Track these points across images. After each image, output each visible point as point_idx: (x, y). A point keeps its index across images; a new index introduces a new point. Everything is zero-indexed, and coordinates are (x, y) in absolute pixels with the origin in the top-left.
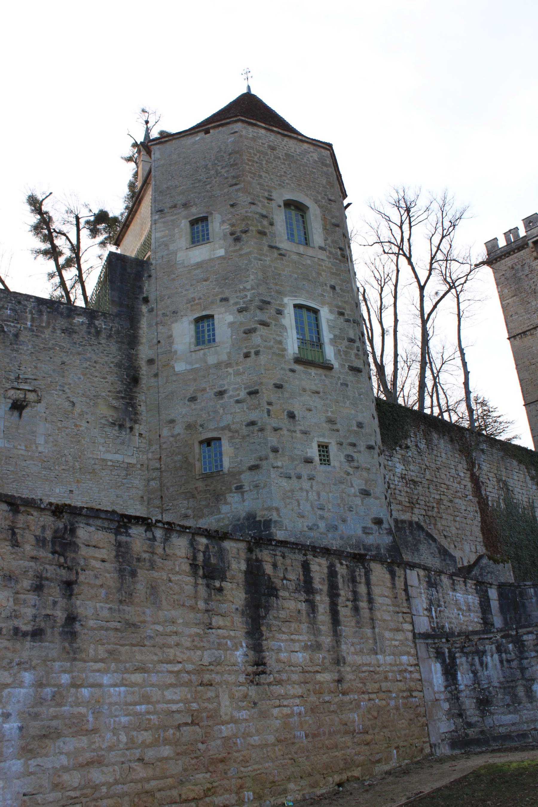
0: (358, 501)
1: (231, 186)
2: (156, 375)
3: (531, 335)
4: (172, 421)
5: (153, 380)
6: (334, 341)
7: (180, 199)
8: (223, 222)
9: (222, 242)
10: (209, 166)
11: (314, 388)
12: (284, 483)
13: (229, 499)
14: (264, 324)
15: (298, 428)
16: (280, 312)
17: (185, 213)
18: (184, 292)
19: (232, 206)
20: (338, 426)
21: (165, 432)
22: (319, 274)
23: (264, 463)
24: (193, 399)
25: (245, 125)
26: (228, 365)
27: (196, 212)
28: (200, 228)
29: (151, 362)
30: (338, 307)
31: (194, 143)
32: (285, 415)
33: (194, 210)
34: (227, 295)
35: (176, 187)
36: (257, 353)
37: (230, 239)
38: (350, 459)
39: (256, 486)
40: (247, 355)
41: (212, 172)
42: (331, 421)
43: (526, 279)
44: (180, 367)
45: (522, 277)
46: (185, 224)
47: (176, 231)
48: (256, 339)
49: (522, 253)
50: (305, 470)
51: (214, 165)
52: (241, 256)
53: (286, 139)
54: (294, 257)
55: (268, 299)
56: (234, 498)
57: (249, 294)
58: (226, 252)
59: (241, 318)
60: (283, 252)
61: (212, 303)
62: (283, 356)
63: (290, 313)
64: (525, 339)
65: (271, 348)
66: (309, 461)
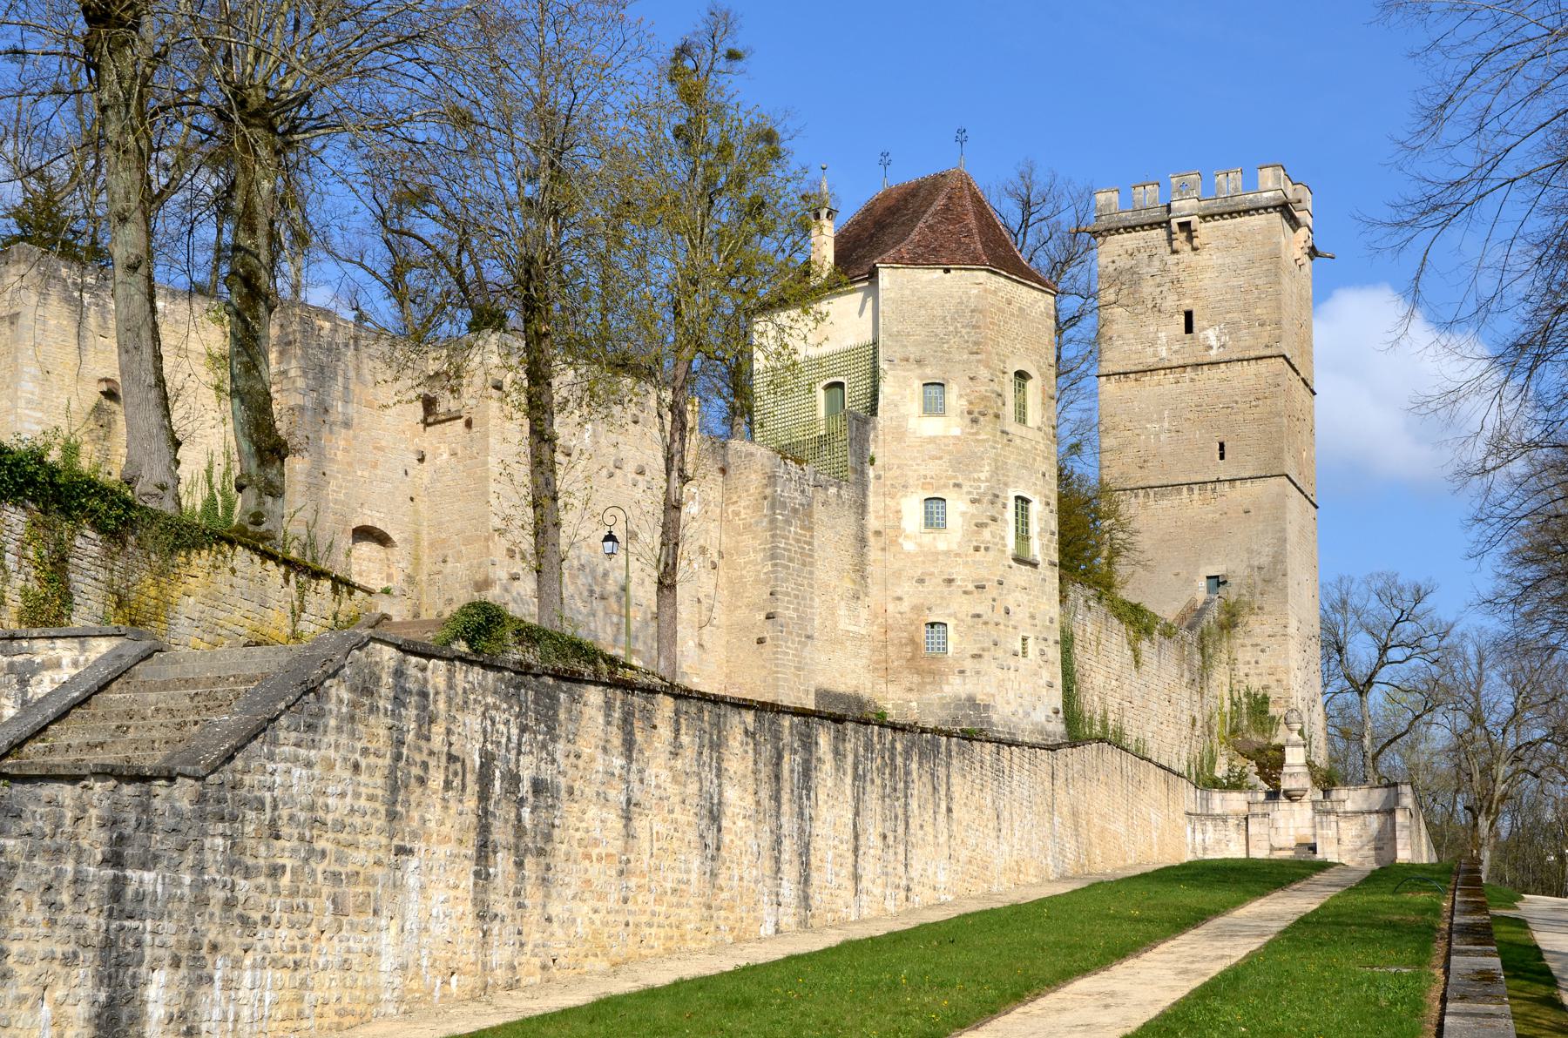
0: (1044, 691)
1: (972, 353)
2: (883, 549)
3: (1136, 380)
4: (899, 599)
5: (880, 553)
6: (1040, 534)
7: (914, 352)
8: (961, 396)
9: (959, 419)
10: (948, 319)
11: (1023, 584)
12: (999, 673)
13: (951, 681)
14: (994, 520)
15: (1012, 623)
16: (1004, 506)
17: (918, 371)
18: (915, 467)
19: (971, 379)
20: (1037, 622)
21: (891, 608)
22: (1035, 460)
23: (986, 654)
24: (921, 581)
25: (989, 274)
26: (958, 555)
27: (932, 373)
28: (933, 394)
29: (878, 533)
30: (1046, 496)
31: (931, 282)
32: (1002, 612)
33: (928, 371)
34: (960, 481)
35: (908, 334)
36: (987, 549)
37: (967, 418)
38: (1043, 653)
39: (978, 673)
40: (977, 549)
41: (951, 328)
42: (1033, 617)
43: (1151, 283)
44: (909, 546)
45: (1145, 276)
46: (917, 385)
47: (908, 391)
48: (986, 534)
49: (1154, 232)
50: (1012, 662)
51: (953, 319)
52: (978, 441)
53: (1021, 286)
54: (1018, 441)
55: (997, 492)
56: (956, 680)
57: (983, 485)
58: (962, 433)
59: (972, 509)
60: (1010, 437)
61: (945, 486)
62: (1004, 552)
63: (1011, 504)
64: (1125, 385)
65: (996, 544)
66: (1016, 655)
